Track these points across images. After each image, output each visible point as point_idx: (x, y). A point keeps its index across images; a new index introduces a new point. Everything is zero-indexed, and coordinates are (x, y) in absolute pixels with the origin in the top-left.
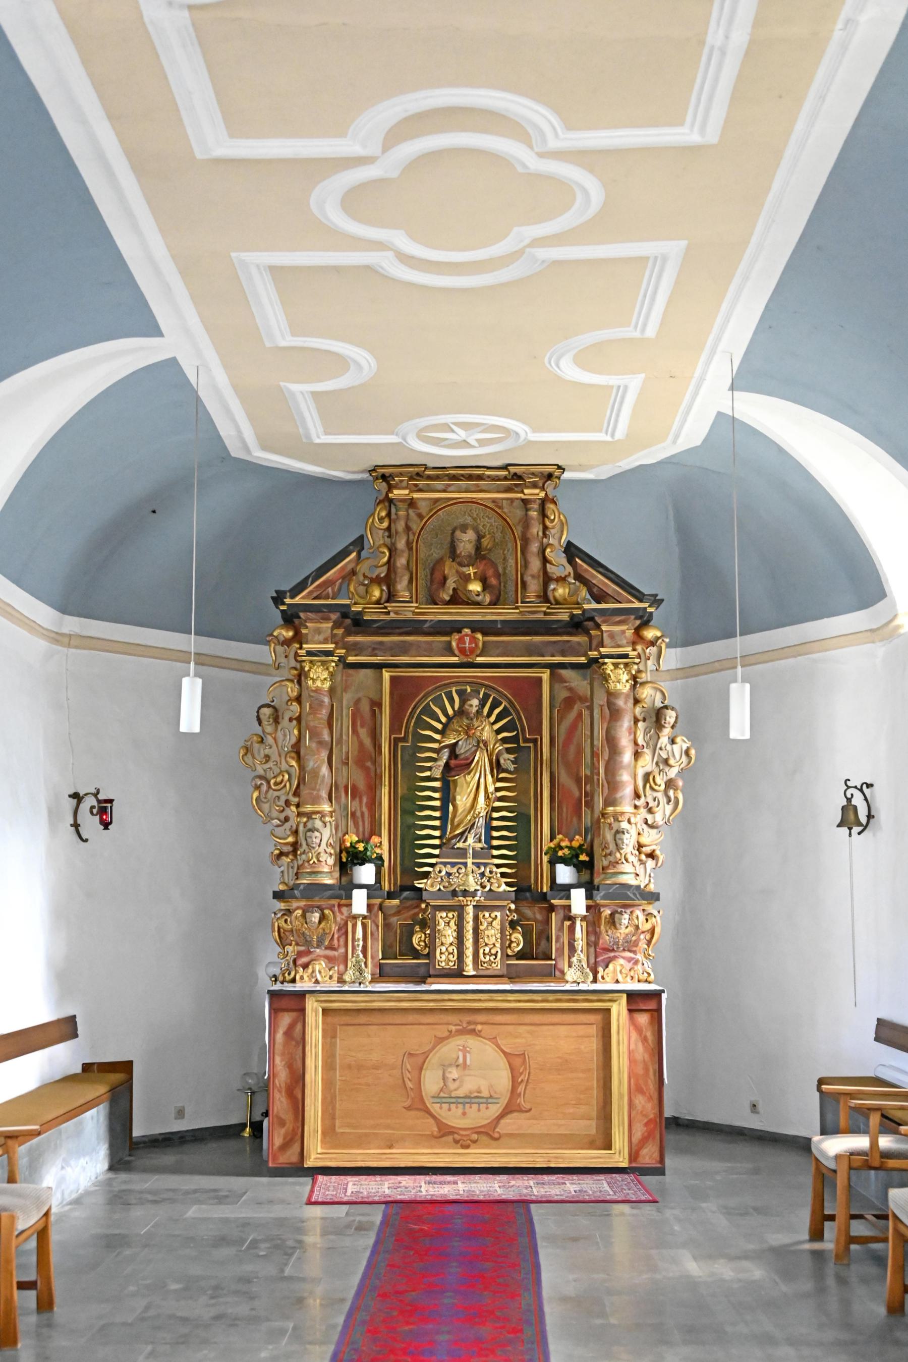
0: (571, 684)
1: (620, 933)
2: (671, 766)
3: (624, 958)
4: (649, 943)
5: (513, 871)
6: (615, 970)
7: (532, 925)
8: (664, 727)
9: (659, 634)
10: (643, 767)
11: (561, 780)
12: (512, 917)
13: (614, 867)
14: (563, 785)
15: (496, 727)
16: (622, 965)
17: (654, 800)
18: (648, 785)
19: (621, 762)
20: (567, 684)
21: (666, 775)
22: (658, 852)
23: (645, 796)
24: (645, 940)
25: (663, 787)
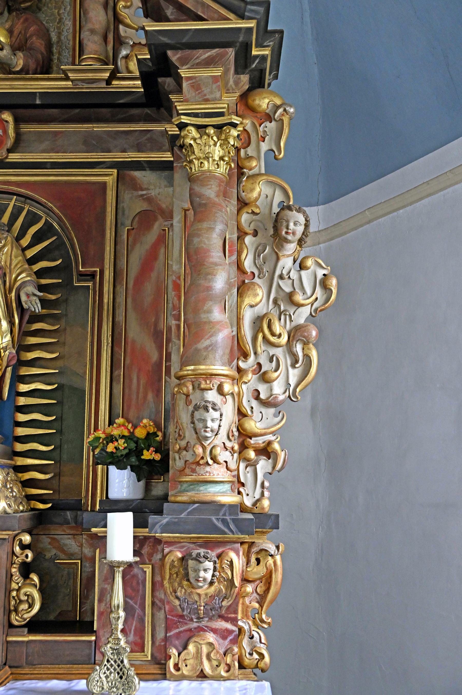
0: (150, 192)
1: (199, 595)
2: (299, 305)
3: (215, 631)
4: (261, 600)
5: (48, 476)
6: (198, 652)
7: (76, 564)
8: (287, 241)
9: (278, 102)
10: (252, 306)
11: (131, 335)
12: (23, 557)
13: (194, 471)
14: (134, 342)
15: (30, 253)
16: (210, 644)
17: (271, 360)
18: (260, 336)
19: (209, 288)
20: (144, 192)
21: (291, 321)
22: (276, 446)
23: (255, 353)
24: (255, 594)
25: (284, 339)
